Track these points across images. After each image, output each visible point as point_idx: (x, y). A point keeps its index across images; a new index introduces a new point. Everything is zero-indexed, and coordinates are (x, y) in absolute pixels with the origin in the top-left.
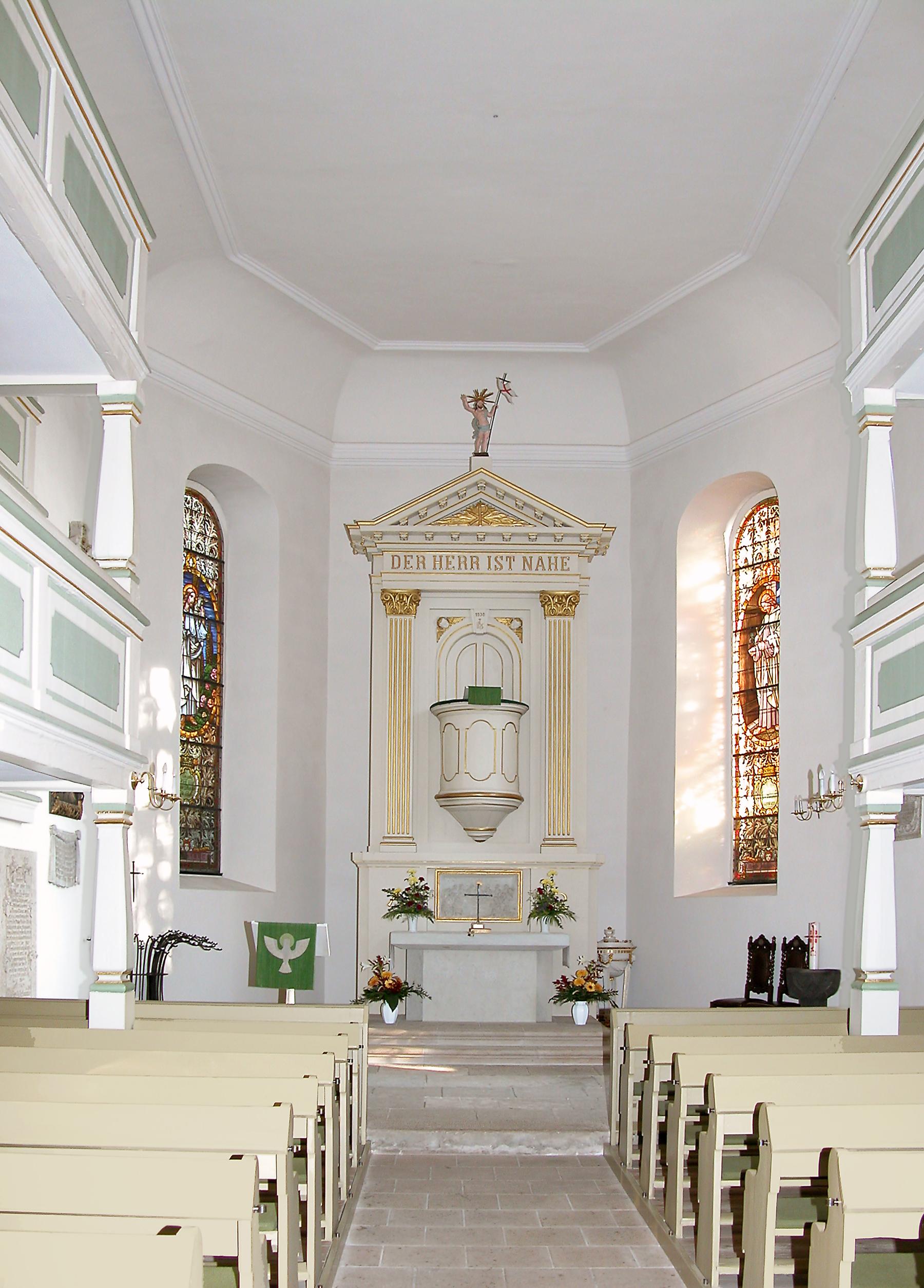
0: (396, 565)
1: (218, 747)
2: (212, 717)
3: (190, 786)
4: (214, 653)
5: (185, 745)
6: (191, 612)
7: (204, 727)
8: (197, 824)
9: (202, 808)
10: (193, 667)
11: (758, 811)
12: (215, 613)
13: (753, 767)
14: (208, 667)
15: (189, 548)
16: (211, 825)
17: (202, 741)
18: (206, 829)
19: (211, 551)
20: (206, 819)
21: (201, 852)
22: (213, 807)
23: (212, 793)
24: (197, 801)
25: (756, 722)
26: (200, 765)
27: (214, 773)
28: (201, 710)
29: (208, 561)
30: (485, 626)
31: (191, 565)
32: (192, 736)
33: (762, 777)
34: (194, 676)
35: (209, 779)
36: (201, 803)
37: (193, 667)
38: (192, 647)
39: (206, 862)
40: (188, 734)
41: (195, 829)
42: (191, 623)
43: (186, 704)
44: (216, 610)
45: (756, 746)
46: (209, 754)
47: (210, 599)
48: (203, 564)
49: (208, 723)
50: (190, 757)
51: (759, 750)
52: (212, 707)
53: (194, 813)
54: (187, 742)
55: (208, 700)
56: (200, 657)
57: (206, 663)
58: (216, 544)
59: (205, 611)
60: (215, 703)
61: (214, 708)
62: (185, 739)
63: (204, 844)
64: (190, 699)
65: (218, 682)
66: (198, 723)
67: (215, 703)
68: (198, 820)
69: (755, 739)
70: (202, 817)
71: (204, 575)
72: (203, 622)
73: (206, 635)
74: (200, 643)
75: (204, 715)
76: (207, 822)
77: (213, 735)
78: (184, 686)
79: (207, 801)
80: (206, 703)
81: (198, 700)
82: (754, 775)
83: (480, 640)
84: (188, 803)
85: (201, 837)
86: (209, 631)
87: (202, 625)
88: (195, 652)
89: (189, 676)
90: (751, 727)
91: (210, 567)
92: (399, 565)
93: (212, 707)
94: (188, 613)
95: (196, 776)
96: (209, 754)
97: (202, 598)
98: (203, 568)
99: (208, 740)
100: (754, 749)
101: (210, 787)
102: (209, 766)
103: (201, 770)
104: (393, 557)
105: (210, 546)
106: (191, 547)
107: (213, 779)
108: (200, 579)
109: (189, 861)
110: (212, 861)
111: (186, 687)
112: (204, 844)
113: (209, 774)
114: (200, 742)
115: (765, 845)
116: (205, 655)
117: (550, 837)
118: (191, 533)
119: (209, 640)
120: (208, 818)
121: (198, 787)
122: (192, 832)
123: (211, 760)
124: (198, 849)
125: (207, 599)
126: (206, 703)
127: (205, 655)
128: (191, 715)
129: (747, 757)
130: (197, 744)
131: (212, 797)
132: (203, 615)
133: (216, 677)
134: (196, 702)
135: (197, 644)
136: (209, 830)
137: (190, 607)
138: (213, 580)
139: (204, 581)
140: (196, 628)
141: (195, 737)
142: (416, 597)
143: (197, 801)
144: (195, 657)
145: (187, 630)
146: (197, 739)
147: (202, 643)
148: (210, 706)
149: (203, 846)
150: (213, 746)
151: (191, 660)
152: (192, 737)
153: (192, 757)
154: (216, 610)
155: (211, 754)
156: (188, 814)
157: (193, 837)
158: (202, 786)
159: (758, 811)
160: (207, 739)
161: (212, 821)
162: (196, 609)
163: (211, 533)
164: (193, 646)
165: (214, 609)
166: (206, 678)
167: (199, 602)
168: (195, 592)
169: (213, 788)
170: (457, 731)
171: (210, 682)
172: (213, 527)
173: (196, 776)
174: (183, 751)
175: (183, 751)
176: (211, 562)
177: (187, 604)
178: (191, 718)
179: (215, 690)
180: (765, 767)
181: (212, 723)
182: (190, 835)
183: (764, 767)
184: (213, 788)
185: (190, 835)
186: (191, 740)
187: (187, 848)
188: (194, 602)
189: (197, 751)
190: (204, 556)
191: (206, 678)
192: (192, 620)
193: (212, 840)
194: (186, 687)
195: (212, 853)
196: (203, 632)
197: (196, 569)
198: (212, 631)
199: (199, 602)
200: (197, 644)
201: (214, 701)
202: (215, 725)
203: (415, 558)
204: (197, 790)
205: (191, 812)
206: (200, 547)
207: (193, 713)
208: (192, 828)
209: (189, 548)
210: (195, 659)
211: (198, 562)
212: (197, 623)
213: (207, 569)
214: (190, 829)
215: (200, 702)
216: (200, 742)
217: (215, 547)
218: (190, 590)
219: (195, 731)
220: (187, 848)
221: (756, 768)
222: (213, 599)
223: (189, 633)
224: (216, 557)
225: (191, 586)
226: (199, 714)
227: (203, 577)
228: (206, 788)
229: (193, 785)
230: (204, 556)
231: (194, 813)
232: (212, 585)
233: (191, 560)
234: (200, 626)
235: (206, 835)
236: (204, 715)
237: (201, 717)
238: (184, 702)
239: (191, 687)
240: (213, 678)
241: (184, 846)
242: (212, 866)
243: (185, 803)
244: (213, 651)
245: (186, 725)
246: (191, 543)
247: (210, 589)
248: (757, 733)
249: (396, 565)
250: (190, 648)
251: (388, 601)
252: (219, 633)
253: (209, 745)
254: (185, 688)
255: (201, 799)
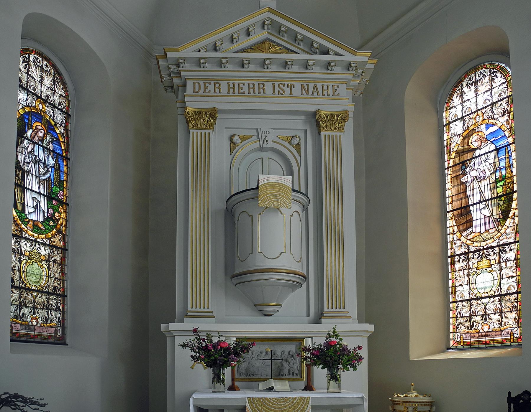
0: (197, 90)
1: (64, 250)
2: (59, 226)
3: (37, 276)
4: (61, 179)
5: (34, 244)
6: (40, 143)
7: (51, 233)
8: (44, 306)
9: (49, 294)
10: (42, 186)
11: (474, 294)
12: (62, 150)
13: (468, 263)
14: (55, 189)
15: (39, 95)
16: (58, 307)
17: (49, 243)
18: (53, 310)
19: (60, 104)
20: (53, 302)
21: (47, 327)
22: (60, 293)
23: (58, 283)
24: (44, 287)
25: (470, 230)
26: (48, 261)
27: (61, 268)
28: (49, 219)
29: (57, 111)
30: (270, 141)
31: (41, 109)
32: (39, 237)
33: (477, 270)
34: (42, 192)
35: (56, 272)
36: (48, 290)
37: (42, 186)
38: (40, 170)
39: (54, 335)
40: (36, 235)
41: (43, 309)
42: (39, 152)
43: (35, 211)
44: (63, 148)
45: (470, 247)
46: (56, 253)
47: (58, 139)
48: (52, 111)
49: (55, 230)
50: (38, 253)
51: (473, 249)
52: (59, 219)
53: (41, 296)
54: (36, 241)
55: (55, 213)
56: (48, 179)
57: (54, 185)
58: (64, 100)
59: (53, 146)
60: (62, 216)
61: (61, 221)
62: (33, 239)
63: (51, 321)
64: (38, 209)
65: (64, 201)
66: (46, 229)
67: (62, 216)
68: (46, 302)
69: (469, 242)
70: (50, 301)
71: (53, 120)
72: (52, 154)
73: (54, 165)
74: (48, 169)
75: (51, 223)
76: (54, 304)
77: (59, 240)
78: (32, 198)
79: (54, 289)
80: (53, 215)
81: (46, 211)
82: (469, 269)
83: (264, 154)
84: (36, 289)
85: (48, 315)
86: (57, 162)
87: (50, 157)
88: (44, 175)
89: (38, 191)
90: (464, 234)
91: (59, 115)
92: (199, 89)
93: (59, 219)
94: (38, 144)
95: (44, 269)
96: (56, 253)
97: (51, 136)
98: (52, 114)
99: (55, 243)
100: (468, 250)
101: (57, 278)
102: (56, 263)
103: (48, 265)
104: (194, 83)
105: (59, 100)
106: (41, 95)
107: (60, 273)
108: (48, 121)
109: (37, 333)
110: (59, 334)
111: (34, 199)
112: (51, 321)
113: (56, 269)
114: (48, 243)
115: (482, 320)
116: (52, 179)
117: (328, 310)
118: (41, 85)
119: (57, 169)
120: (55, 301)
121: (45, 277)
122: (40, 311)
123: (58, 258)
124: (45, 325)
125: (55, 138)
126: (53, 215)
127: (52, 179)
128: (39, 221)
129: (462, 257)
130: (45, 244)
131: (59, 286)
132: (51, 148)
133: (62, 197)
134: (44, 212)
135: (46, 169)
136: (56, 311)
137: (39, 140)
138: (61, 126)
139: (53, 123)
140: (44, 157)
141: (42, 239)
142: (212, 114)
143: (44, 287)
144: (44, 178)
145: (36, 156)
146: (45, 240)
147: (50, 170)
148: (57, 218)
149: (51, 323)
150: (60, 248)
151: (40, 180)
152: (39, 238)
153: (41, 254)
154: (63, 148)
155: (58, 254)
156: (36, 297)
157: (41, 315)
158: (49, 277)
159: (474, 294)
160: (54, 242)
161: (59, 304)
162: (45, 142)
163: (60, 91)
164: (42, 170)
165: (61, 146)
166: (53, 196)
167: (48, 138)
168: (44, 130)
169: (60, 280)
170: (250, 218)
171: (57, 200)
172: (61, 88)
173: (44, 269)
174: (32, 248)
175: (32, 248)
176: (59, 112)
177: (36, 136)
178: (39, 223)
179: (62, 207)
180: (480, 261)
181: (59, 232)
182: (38, 313)
183: (478, 261)
184: (60, 280)
185: (38, 313)
186: (38, 240)
187: (34, 323)
188: (43, 137)
189: (45, 250)
190: (54, 107)
191: (53, 196)
192: (41, 152)
193: (59, 319)
194: (34, 199)
195: (58, 329)
196: (51, 161)
197: (45, 113)
198: (60, 163)
199: (48, 138)
200: (46, 169)
201: (61, 215)
202: (61, 233)
203: (212, 84)
204: (45, 280)
205: (40, 295)
206: (50, 98)
207: (41, 220)
208: (40, 308)
209: (39, 95)
210: (43, 180)
211: (47, 109)
212: (46, 153)
213: (55, 116)
214: (37, 308)
215: (48, 213)
216: (48, 243)
217: (63, 102)
218: (40, 127)
219: (43, 234)
220: (34, 323)
221: (471, 264)
222: (61, 139)
223: (37, 158)
224: (64, 110)
225: (40, 124)
226: (47, 222)
227: (52, 121)
228: (53, 279)
229: (41, 275)
230: (54, 107)
231: (41, 296)
232: (60, 129)
233: (41, 104)
234: (48, 156)
235: (53, 314)
236: (51, 223)
237: (49, 225)
238: (33, 210)
239: (39, 200)
240: (60, 197)
241: (32, 322)
242: (58, 338)
243: (32, 288)
244: (60, 178)
245: (34, 228)
246: (41, 92)
247: (58, 131)
248: (471, 237)
249: (197, 90)
250: (39, 170)
251: (190, 116)
252: (66, 166)
253: (57, 247)
254: (33, 200)
255: (48, 287)
